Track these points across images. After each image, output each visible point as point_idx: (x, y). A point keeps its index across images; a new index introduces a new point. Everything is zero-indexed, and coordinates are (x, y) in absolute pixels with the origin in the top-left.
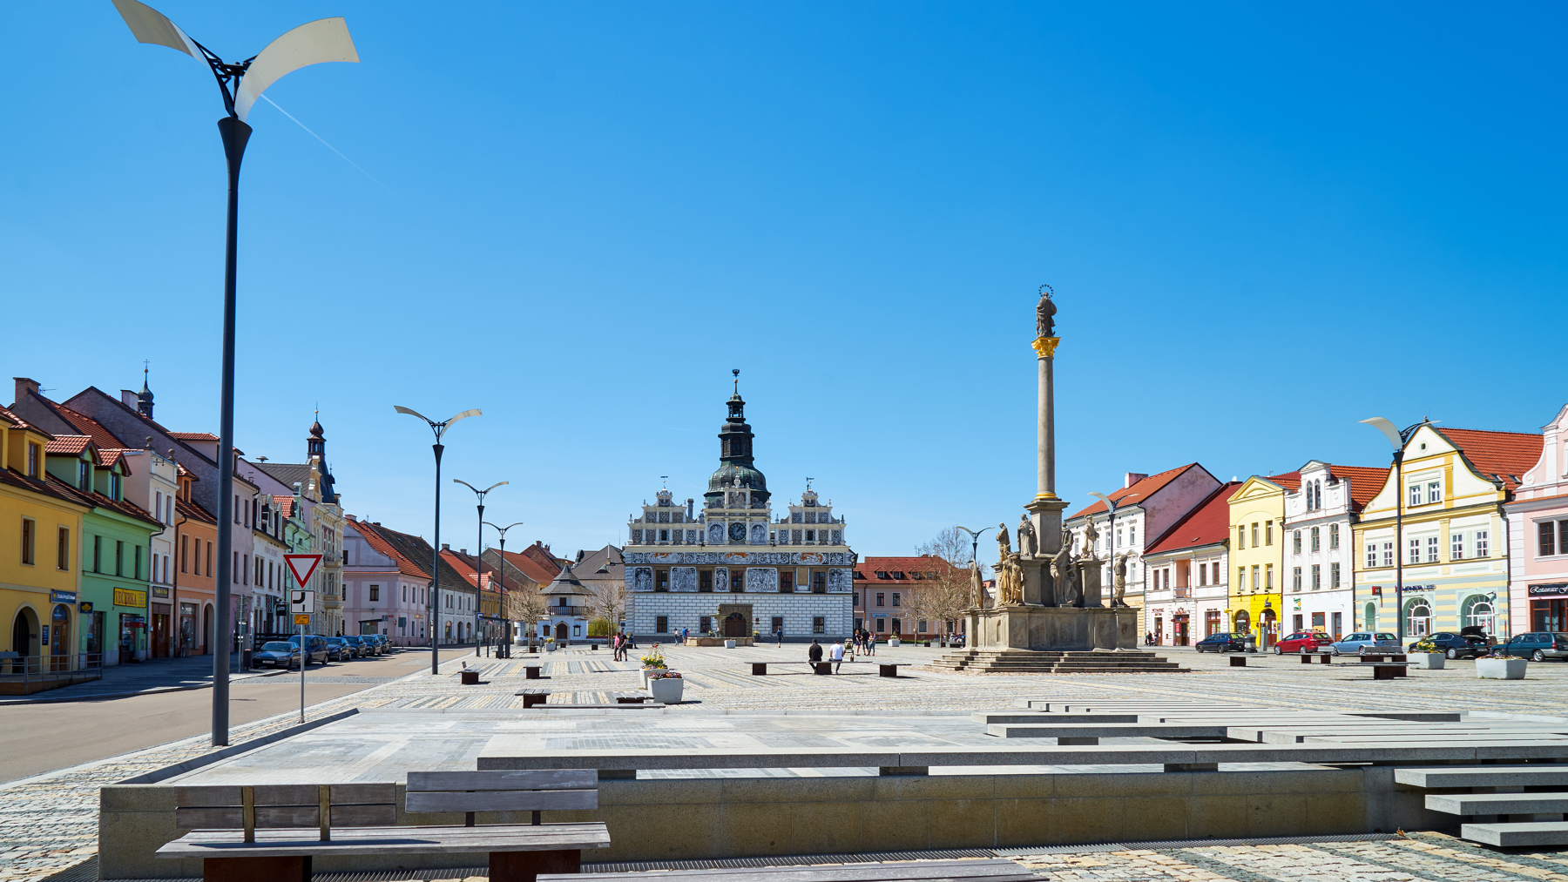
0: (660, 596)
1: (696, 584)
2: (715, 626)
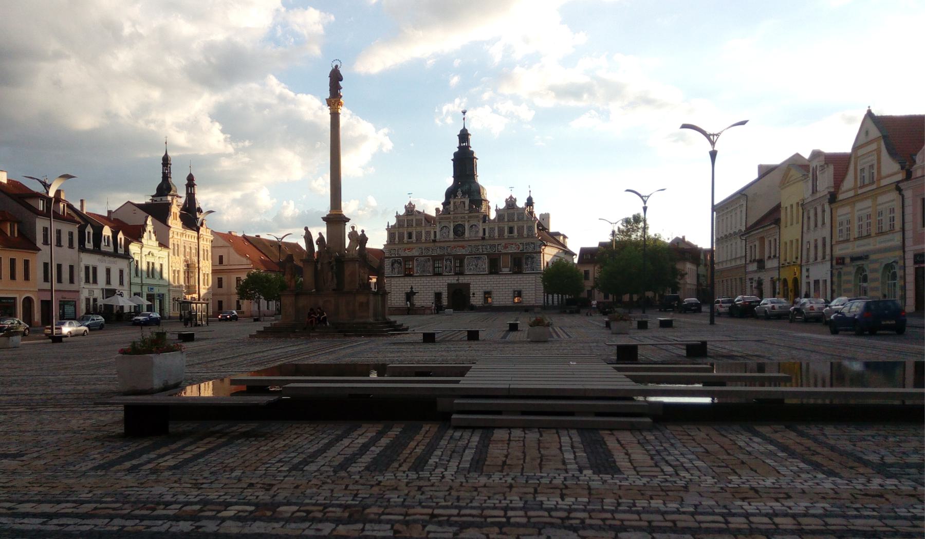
0: (407, 279)
1: (431, 269)
2: (445, 302)
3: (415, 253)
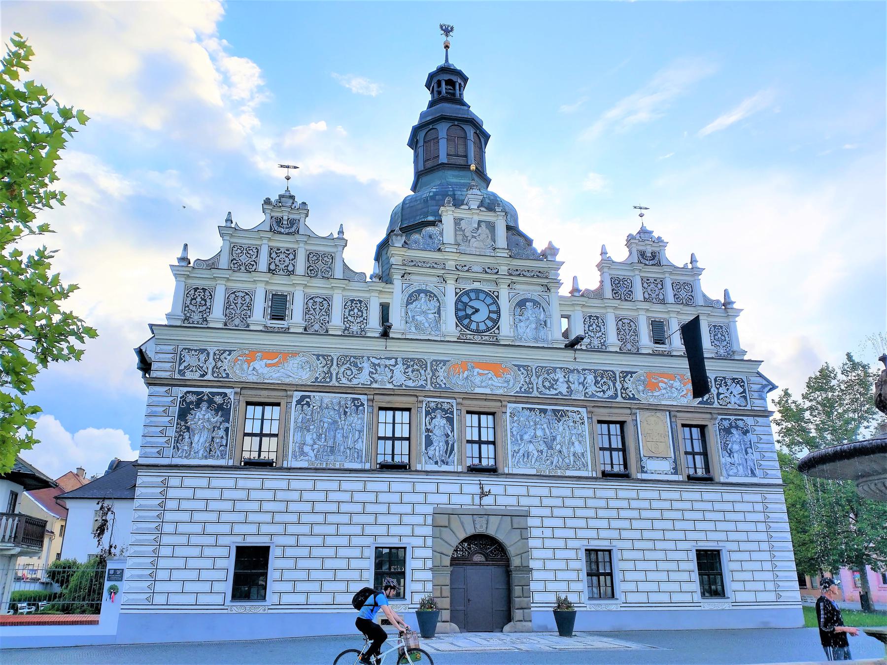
3: (297, 372)
